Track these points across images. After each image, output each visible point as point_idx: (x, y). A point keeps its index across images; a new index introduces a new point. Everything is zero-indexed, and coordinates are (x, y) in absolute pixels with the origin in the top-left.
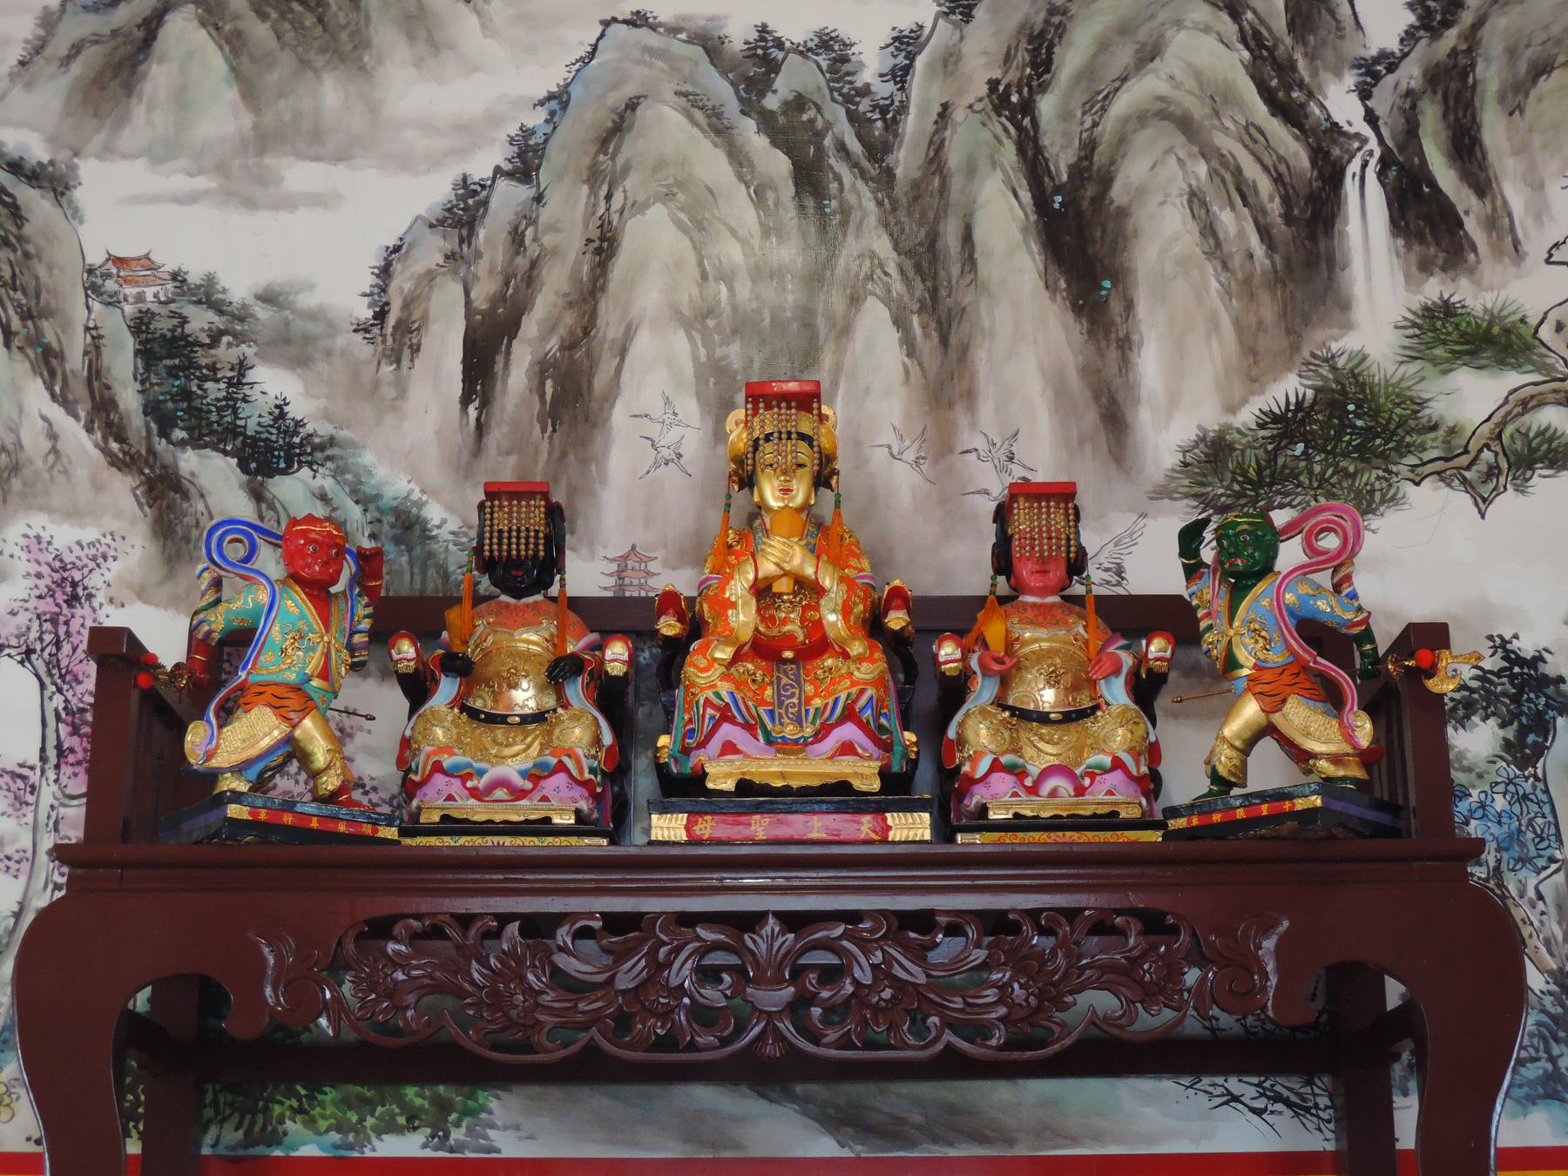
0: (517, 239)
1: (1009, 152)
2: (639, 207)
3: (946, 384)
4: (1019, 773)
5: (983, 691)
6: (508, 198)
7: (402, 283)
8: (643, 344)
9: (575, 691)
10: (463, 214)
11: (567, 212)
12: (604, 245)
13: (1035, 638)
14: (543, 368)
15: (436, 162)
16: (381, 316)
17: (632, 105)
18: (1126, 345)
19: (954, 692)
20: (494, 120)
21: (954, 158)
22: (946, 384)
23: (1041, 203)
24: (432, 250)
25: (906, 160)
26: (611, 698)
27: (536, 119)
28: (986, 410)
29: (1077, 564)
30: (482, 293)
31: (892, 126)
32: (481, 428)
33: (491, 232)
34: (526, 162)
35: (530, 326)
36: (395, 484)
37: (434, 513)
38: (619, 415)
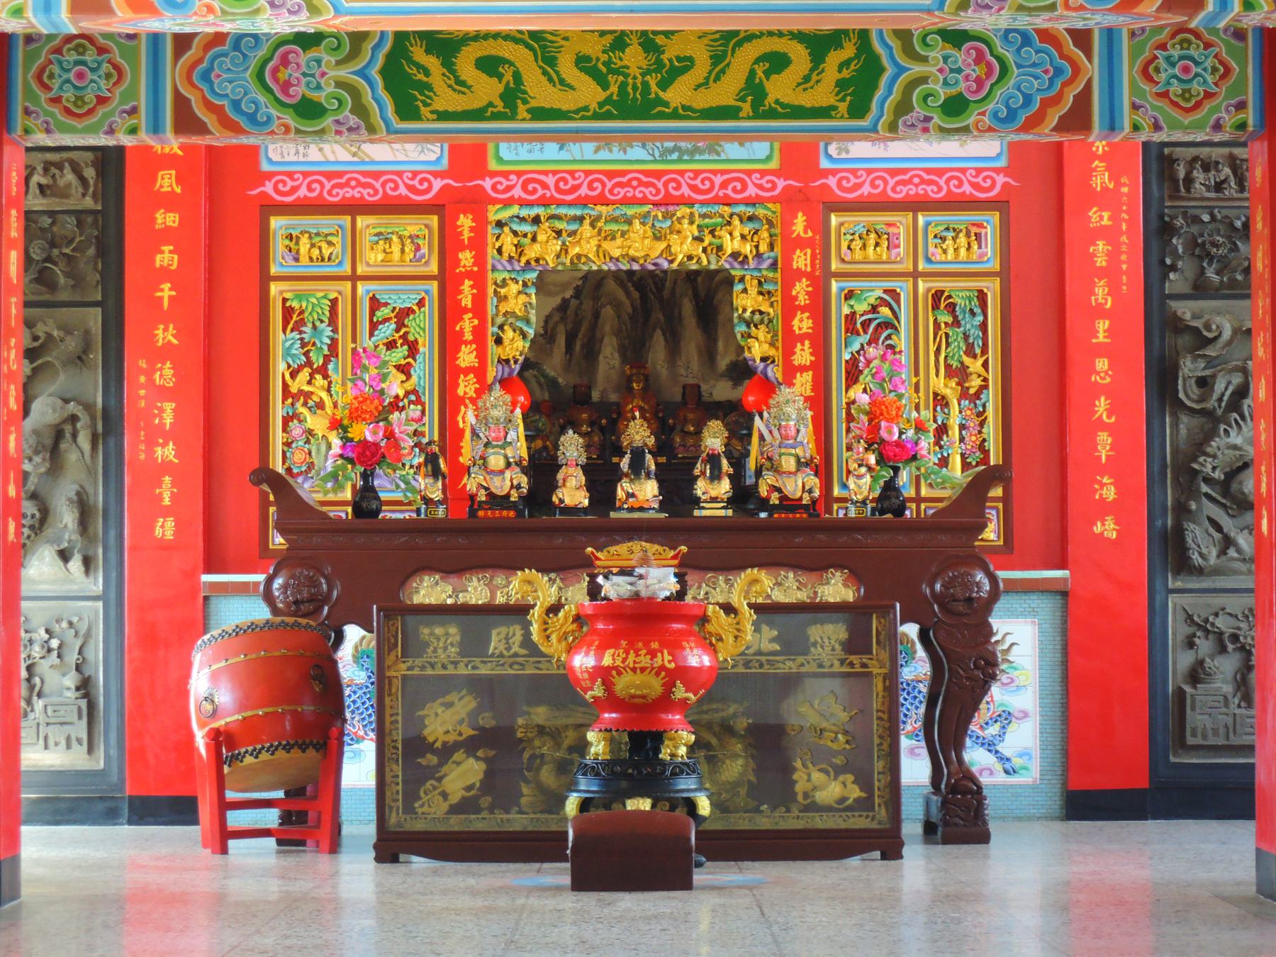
0: (576, 314)
1: (690, 292)
2: (605, 306)
3: (674, 349)
4: (684, 446)
5: (678, 428)
6: (574, 303)
7: (551, 325)
8: (606, 340)
9: (596, 429)
10: (563, 307)
11: (588, 305)
12: (597, 315)
13: (690, 416)
14: (583, 346)
15: (556, 294)
16: (546, 332)
17: (603, 279)
18: (715, 341)
19: (672, 429)
20: (569, 283)
21: (678, 292)
22: (674, 349)
23: (697, 304)
24: (556, 318)
25: (666, 293)
26: (602, 429)
27: (580, 283)
28: (683, 357)
29: (700, 395)
30: (570, 326)
31: (663, 285)
32: (570, 360)
33: (570, 312)
34: (578, 293)
35: (580, 336)
36: (552, 374)
37: (560, 380)
38: (601, 358)
